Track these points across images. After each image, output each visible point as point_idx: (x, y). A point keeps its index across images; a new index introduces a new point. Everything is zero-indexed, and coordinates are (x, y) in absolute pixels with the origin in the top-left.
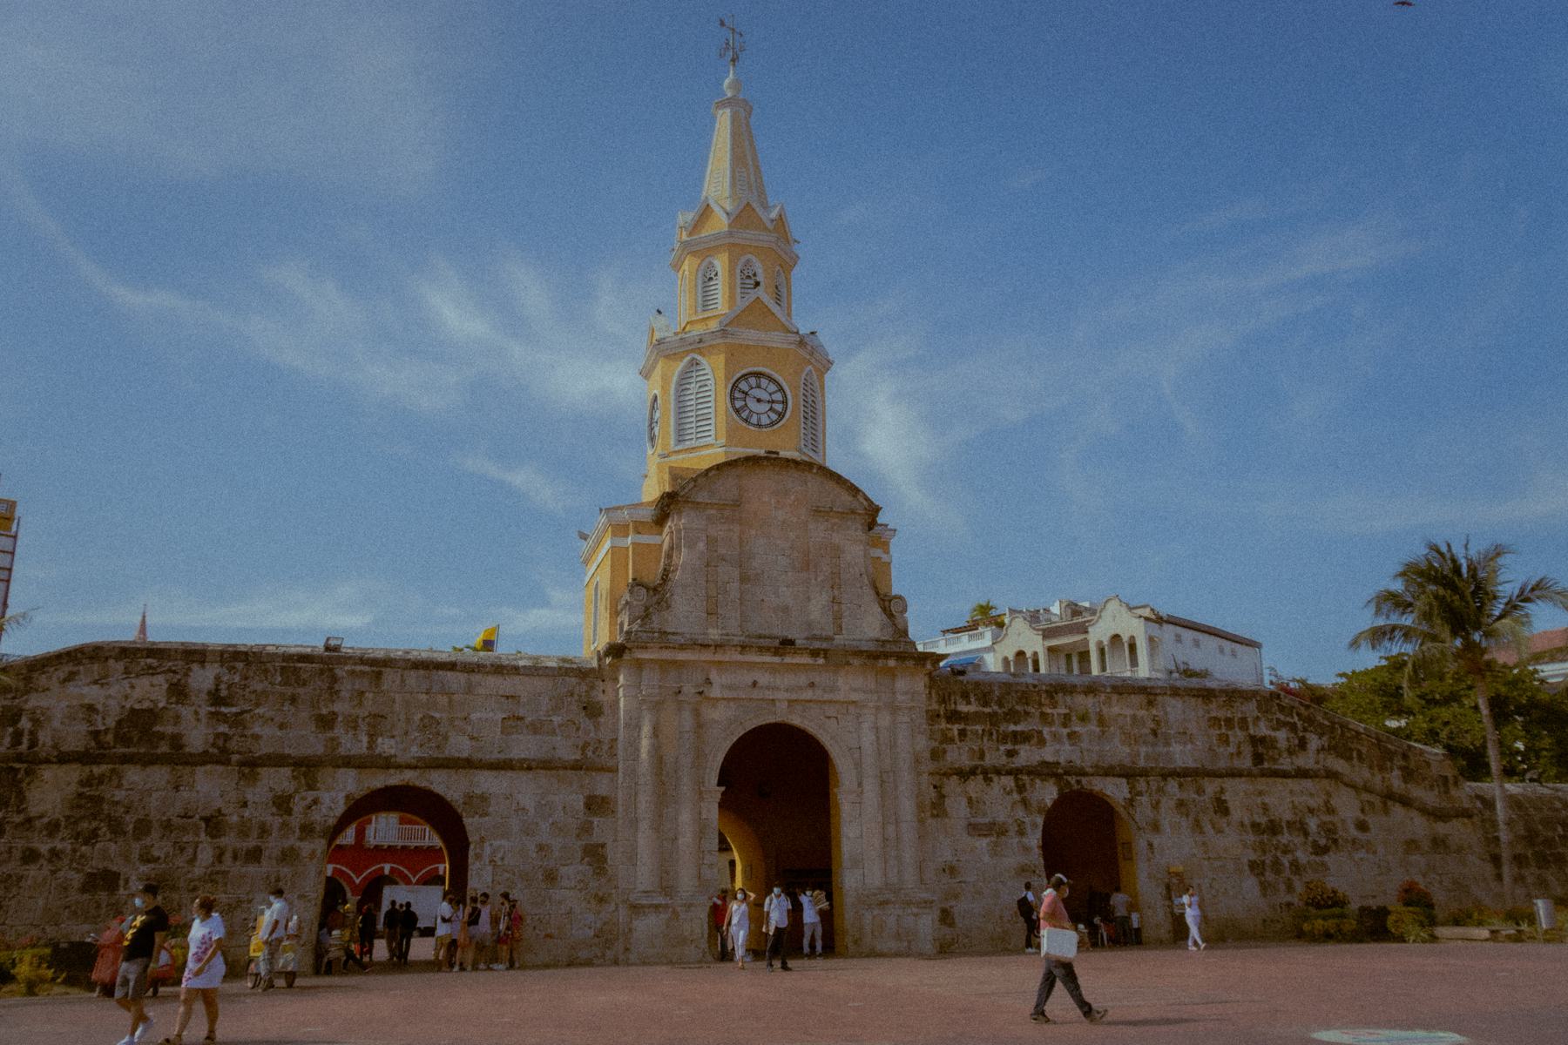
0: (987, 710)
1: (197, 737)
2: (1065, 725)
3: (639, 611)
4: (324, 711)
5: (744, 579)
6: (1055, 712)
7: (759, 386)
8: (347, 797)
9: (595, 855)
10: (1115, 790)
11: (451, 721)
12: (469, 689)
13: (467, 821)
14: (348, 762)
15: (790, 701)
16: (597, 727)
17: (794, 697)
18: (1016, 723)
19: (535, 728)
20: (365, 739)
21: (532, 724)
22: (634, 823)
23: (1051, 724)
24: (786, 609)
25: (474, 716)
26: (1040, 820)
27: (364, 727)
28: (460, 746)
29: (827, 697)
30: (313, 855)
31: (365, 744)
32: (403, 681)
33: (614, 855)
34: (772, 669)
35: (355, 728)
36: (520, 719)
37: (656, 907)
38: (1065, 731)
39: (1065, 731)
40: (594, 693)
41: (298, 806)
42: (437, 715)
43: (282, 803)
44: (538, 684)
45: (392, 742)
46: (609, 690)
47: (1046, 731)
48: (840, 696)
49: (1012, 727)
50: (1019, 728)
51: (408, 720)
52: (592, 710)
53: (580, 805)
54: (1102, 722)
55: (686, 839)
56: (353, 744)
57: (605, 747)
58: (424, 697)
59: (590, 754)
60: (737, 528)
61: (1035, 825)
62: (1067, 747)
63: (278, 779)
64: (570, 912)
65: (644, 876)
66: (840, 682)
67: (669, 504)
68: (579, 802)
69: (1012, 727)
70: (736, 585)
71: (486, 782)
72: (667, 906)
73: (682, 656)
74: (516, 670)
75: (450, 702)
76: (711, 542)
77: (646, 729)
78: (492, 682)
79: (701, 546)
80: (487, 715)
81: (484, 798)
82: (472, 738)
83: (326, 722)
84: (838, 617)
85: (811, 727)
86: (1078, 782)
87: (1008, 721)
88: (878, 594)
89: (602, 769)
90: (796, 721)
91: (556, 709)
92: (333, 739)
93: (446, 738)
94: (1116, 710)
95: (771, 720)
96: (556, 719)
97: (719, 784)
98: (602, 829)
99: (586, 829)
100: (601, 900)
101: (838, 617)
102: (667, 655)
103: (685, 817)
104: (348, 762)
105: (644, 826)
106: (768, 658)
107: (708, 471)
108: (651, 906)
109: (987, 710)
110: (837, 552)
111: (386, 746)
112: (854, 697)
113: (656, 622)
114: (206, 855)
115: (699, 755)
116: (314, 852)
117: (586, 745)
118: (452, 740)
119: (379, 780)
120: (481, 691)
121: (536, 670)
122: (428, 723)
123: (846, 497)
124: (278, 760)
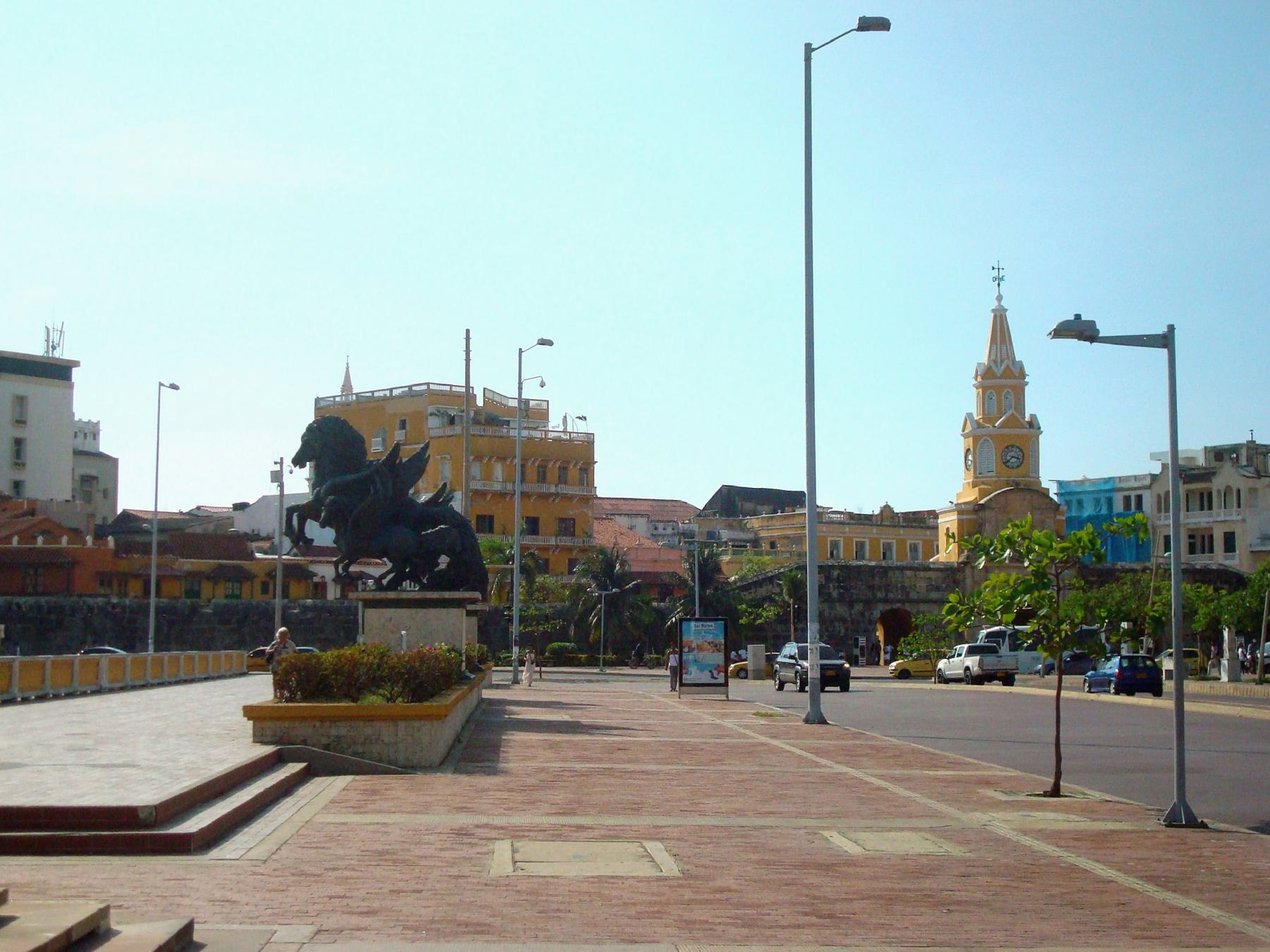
1: (835, 594)
14: (880, 601)
28: (913, 595)
41: (867, 614)
43: (862, 614)
44: (939, 574)
56: (880, 595)
63: (859, 607)
74: (930, 569)
78: (922, 574)
80: (922, 585)
83: (871, 588)
104: (880, 601)
111: (891, 596)
114: (843, 631)
119: (888, 607)
121: (938, 570)
122: (903, 587)
124: (859, 601)
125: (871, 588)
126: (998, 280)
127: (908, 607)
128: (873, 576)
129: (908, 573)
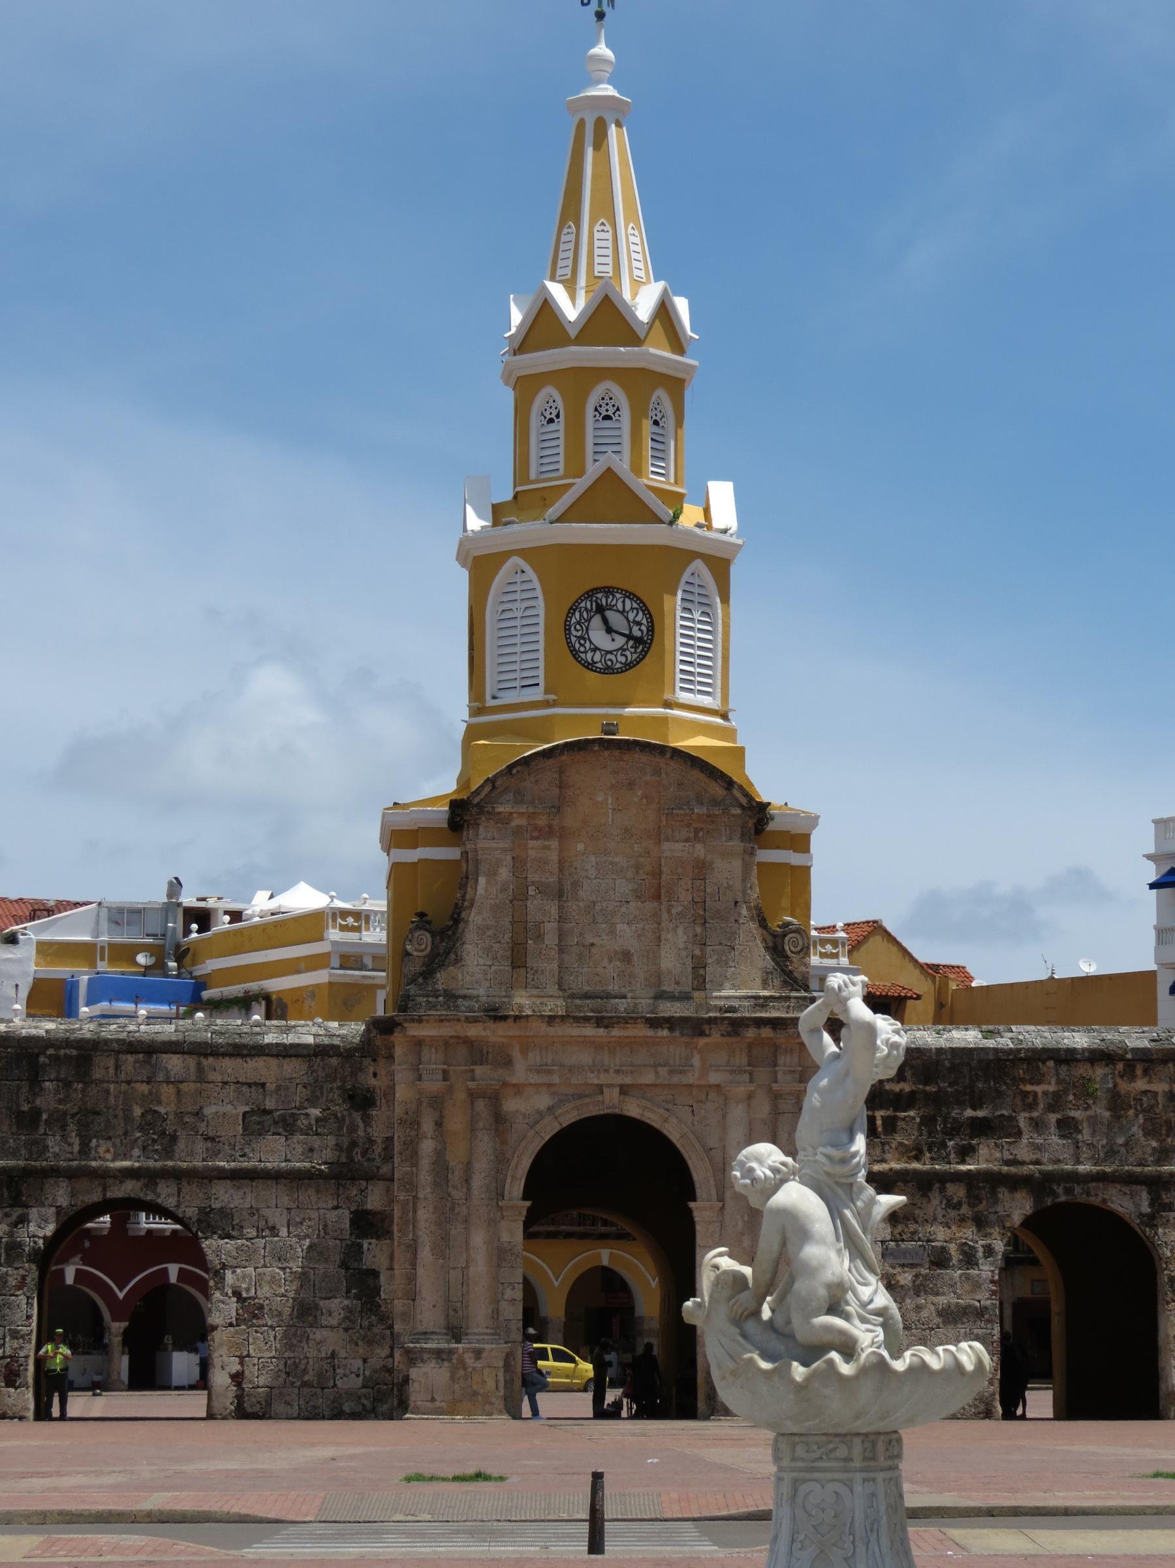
0: (931, 1089)
2: (1051, 1108)
3: (415, 967)
4: (25, 1107)
5: (562, 919)
6: (1039, 1089)
8: (58, 1214)
9: (364, 1285)
10: (1127, 1204)
11: (180, 1115)
12: (201, 1076)
13: (205, 1244)
15: (624, 1090)
16: (367, 1120)
17: (628, 1080)
18: (974, 1109)
19: (288, 1125)
20: (76, 1142)
21: (283, 1119)
22: (413, 1249)
23: (1031, 1107)
24: (626, 956)
25: (209, 1111)
26: (999, 1246)
27: (72, 1127)
29: (675, 1079)
30: (21, 1285)
31: (76, 1148)
32: (117, 1067)
33: (390, 1287)
34: (597, 1046)
35: (63, 1128)
36: (270, 1112)
37: (438, 1354)
38: (1053, 1118)
39: (1053, 1118)
40: (361, 1077)
42: (162, 1110)
44: (292, 1068)
45: (109, 1143)
46: (382, 1072)
47: (1022, 1119)
48: (690, 1079)
49: (969, 1113)
50: (980, 1114)
51: (128, 1118)
52: (362, 1101)
53: (346, 1224)
54: (1117, 1103)
55: (480, 1267)
57: (378, 1149)
58: (144, 1088)
59: (358, 1157)
60: (554, 843)
61: (989, 1251)
62: (1055, 1139)
64: (333, 1355)
65: (429, 1314)
66: (696, 1061)
67: (462, 813)
68: (342, 1219)
69: (969, 1113)
70: (555, 925)
71: (225, 1196)
72: (451, 1352)
73: (474, 1031)
75: (179, 1092)
76: (519, 864)
77: (428, 1126)
78: (228, 1064)
79: (504, 873)
80: (225, 1109)
81: (226, 1213)
82: (207, 1138)
83: (29, 1120)
84: (699, 966)
85: (653, 1118)
86: (1069, 1191)
87: (961, 1104)
88: (763, 923)
89: (370, 1177)
90: (633, 1109)
91: (313, 1101)
92: (35, 1142)
93: (174, 1138)
94: (1141, 1084)
95: (592, 1110)
96: (315, 1112)
97: (524, 1198)
98: (374, 1253)
99: (353, 1252)
100: (370, 1343)
101: (699, 966)
102: (447, 1031)
103: (478, 1239)
105: (425, 1254)
106: (589, 1031)
107: (510, 768)
108: (429, 1351)
109: (931, 1089)
110: (701, 869)
112: (714, 1078)
113: (442, 980)
115: (501, 1161)
116: (24, 1278)
117: (354, 1144)
118: (181, 1144)
120: (215, 1077)
122: (151, 1120)
123: (718, 790)
125: (29, 1120)
127: (166, 1194)
128: (35, 1081)
129: (174, 1063)
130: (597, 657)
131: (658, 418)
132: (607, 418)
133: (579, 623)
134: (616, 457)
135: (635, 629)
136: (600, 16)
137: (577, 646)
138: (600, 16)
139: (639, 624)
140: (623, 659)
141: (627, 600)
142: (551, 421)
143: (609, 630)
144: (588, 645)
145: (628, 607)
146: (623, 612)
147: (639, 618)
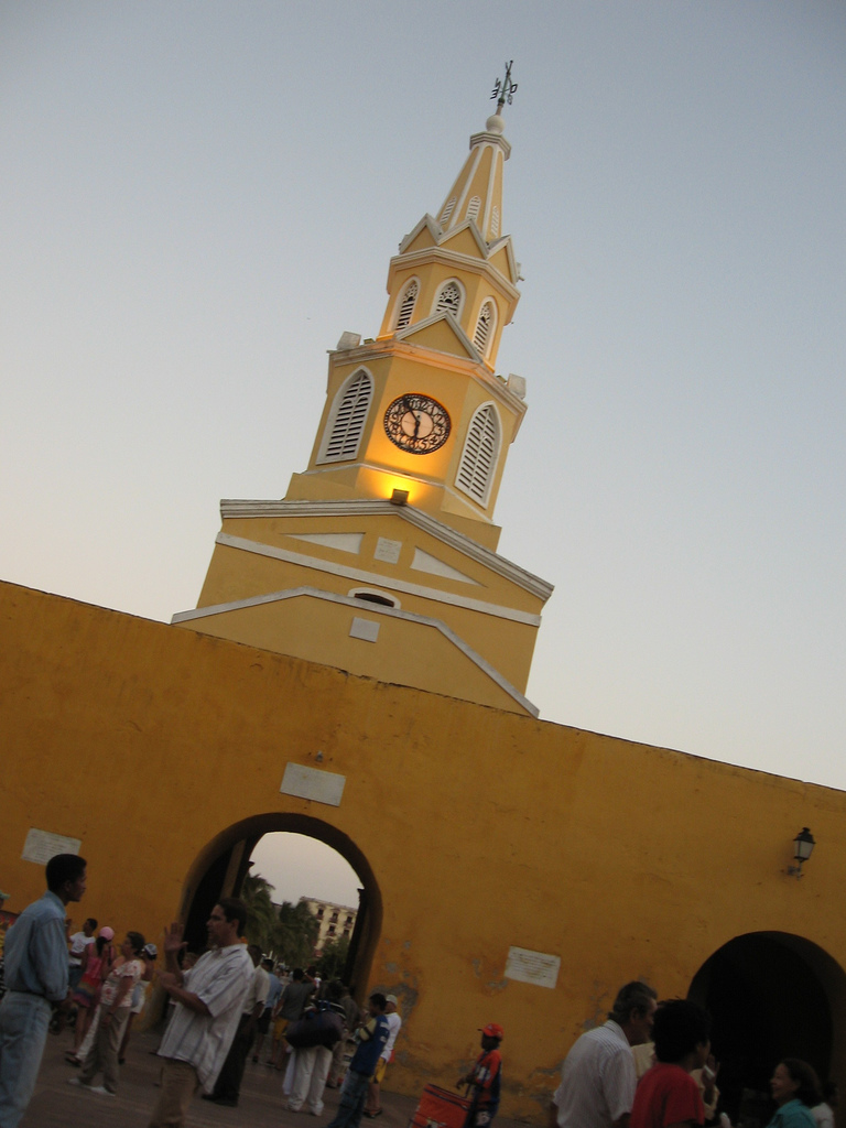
7: (421, 409)
126: (503, 93)
130: (404, 439)
131: (486, 317)
132: (449, 301)
133: (396, 413)
134: (452, 312)
135: (437, 431)
136: (501, 101)
137: (391, 429)
138: (501, 101)
139: (440, 425)
140: (423, 446)
141: (436, 408)
142: (411, 299)
143: (417, 424)
144: (399, 429)
145: (435, 413)
146: (430, 415)
147: (442, 421)
